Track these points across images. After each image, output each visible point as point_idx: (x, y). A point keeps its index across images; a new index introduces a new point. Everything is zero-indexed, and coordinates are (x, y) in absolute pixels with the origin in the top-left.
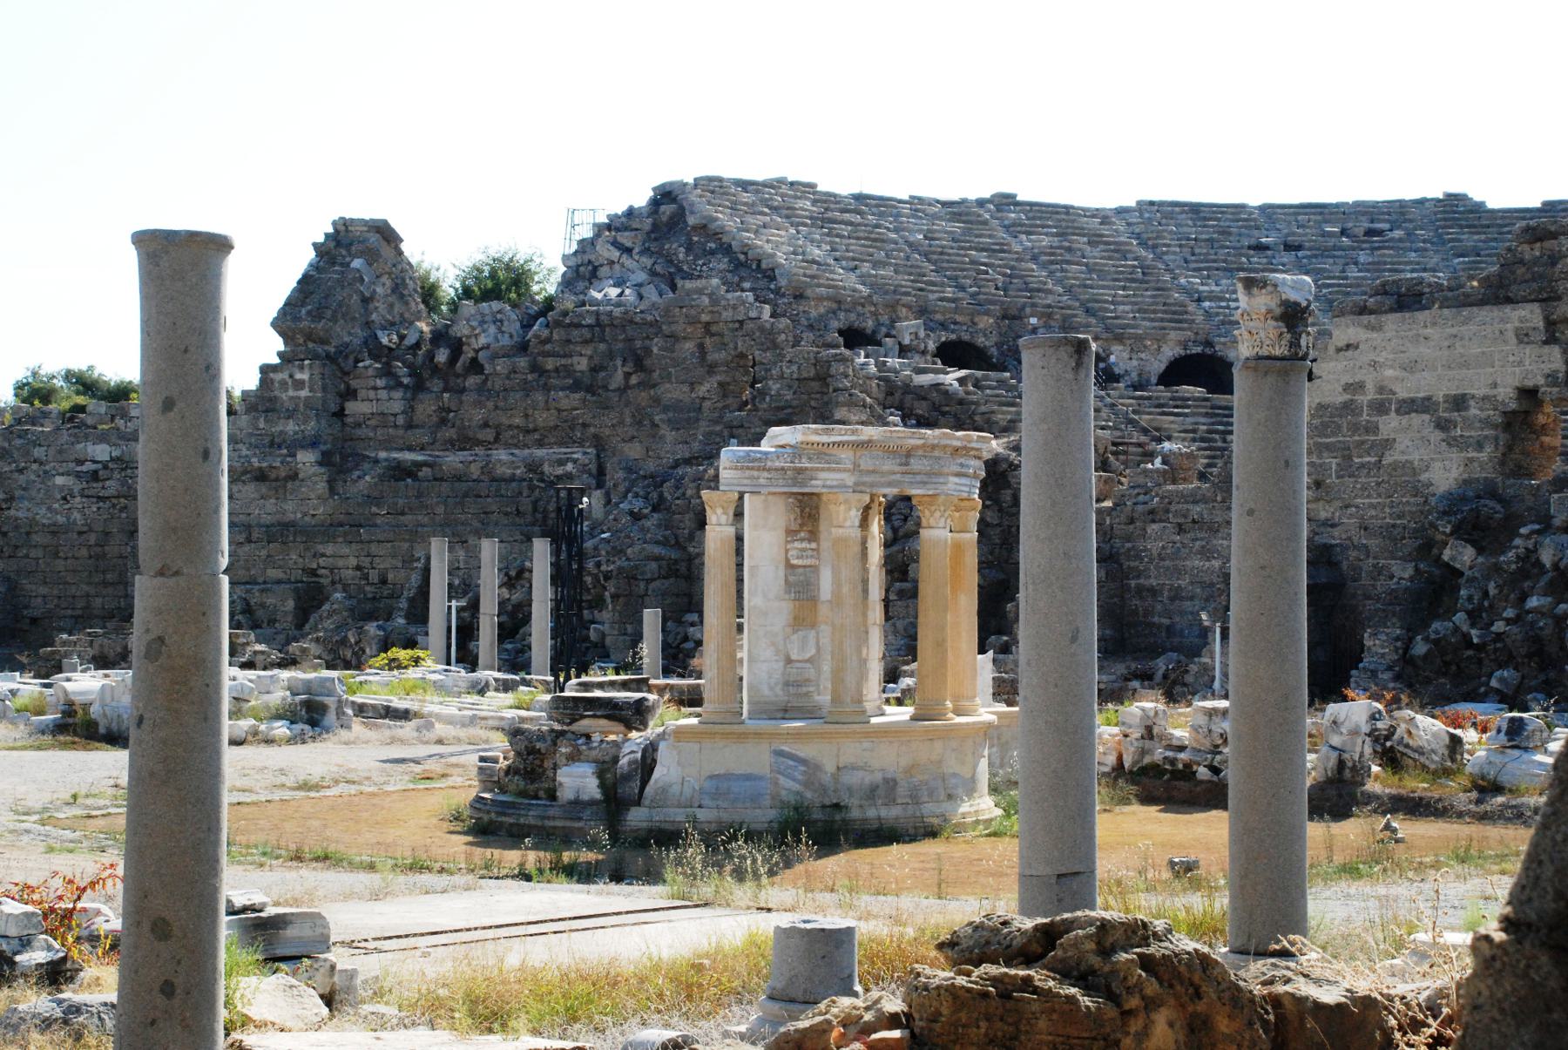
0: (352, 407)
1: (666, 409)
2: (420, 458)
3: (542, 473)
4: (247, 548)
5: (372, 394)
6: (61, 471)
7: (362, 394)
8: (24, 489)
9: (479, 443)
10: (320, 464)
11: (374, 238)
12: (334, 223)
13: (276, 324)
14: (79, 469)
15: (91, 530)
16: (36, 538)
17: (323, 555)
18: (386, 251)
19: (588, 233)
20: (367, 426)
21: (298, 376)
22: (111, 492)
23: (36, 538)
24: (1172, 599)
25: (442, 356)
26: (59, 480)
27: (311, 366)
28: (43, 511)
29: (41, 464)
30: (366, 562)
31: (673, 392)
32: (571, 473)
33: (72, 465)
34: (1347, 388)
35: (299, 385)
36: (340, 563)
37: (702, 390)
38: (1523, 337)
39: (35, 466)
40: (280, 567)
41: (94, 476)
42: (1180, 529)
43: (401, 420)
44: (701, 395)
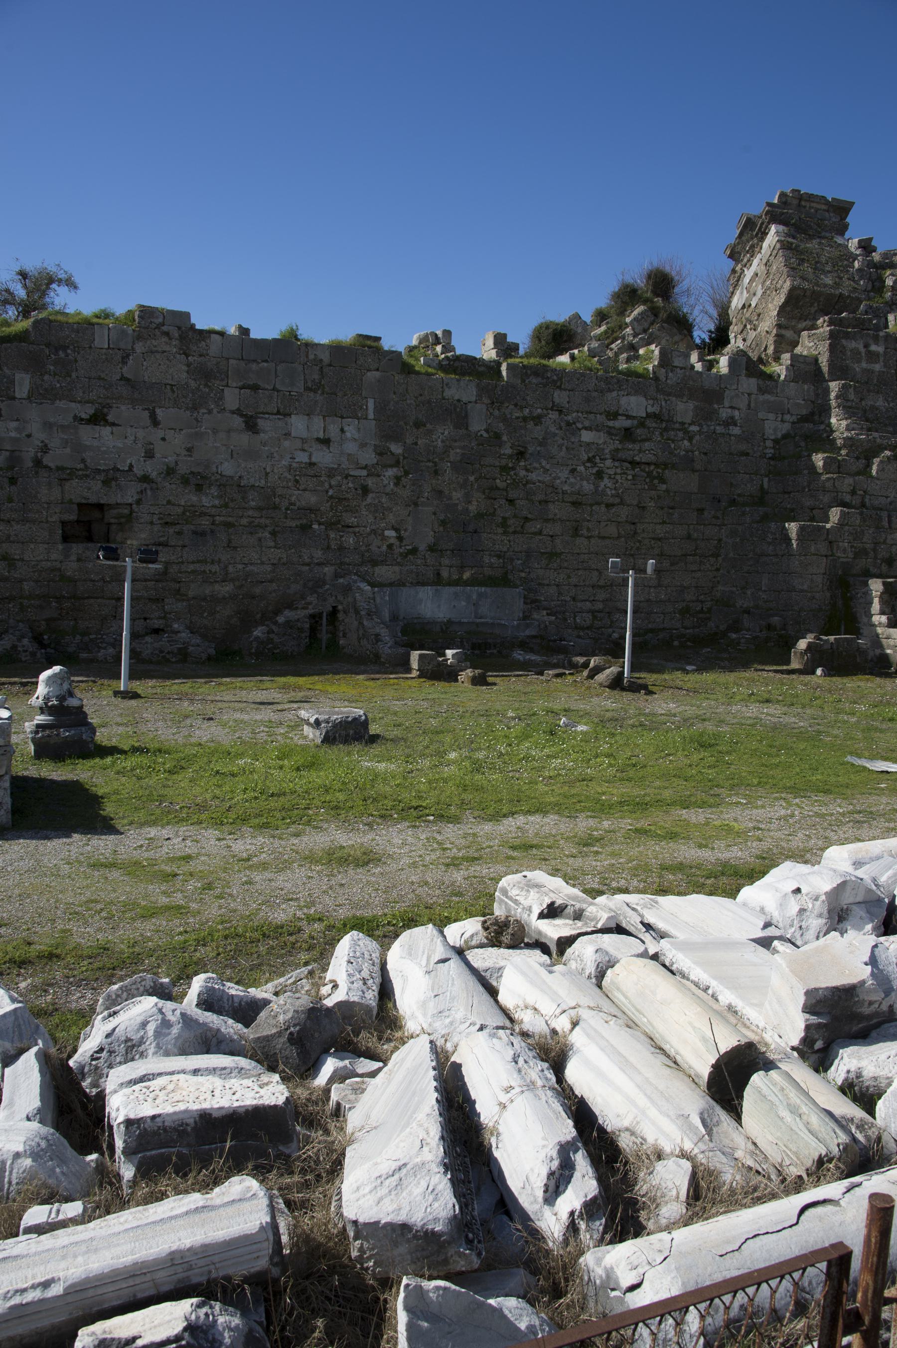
6: (587, 424)
8: (541, 444)
12: (783, 195)
14: (611, 424)
15: (622, 503)
16: (554, 509)
21: (873, 348)
22: (651, 458)
23: (554, 509)
26: (587, 436)
28: (564, 474)
29: (560, 412)
33: (601, 418)
35: (872, 357)
39: (554, 415)
41: (628, 434)
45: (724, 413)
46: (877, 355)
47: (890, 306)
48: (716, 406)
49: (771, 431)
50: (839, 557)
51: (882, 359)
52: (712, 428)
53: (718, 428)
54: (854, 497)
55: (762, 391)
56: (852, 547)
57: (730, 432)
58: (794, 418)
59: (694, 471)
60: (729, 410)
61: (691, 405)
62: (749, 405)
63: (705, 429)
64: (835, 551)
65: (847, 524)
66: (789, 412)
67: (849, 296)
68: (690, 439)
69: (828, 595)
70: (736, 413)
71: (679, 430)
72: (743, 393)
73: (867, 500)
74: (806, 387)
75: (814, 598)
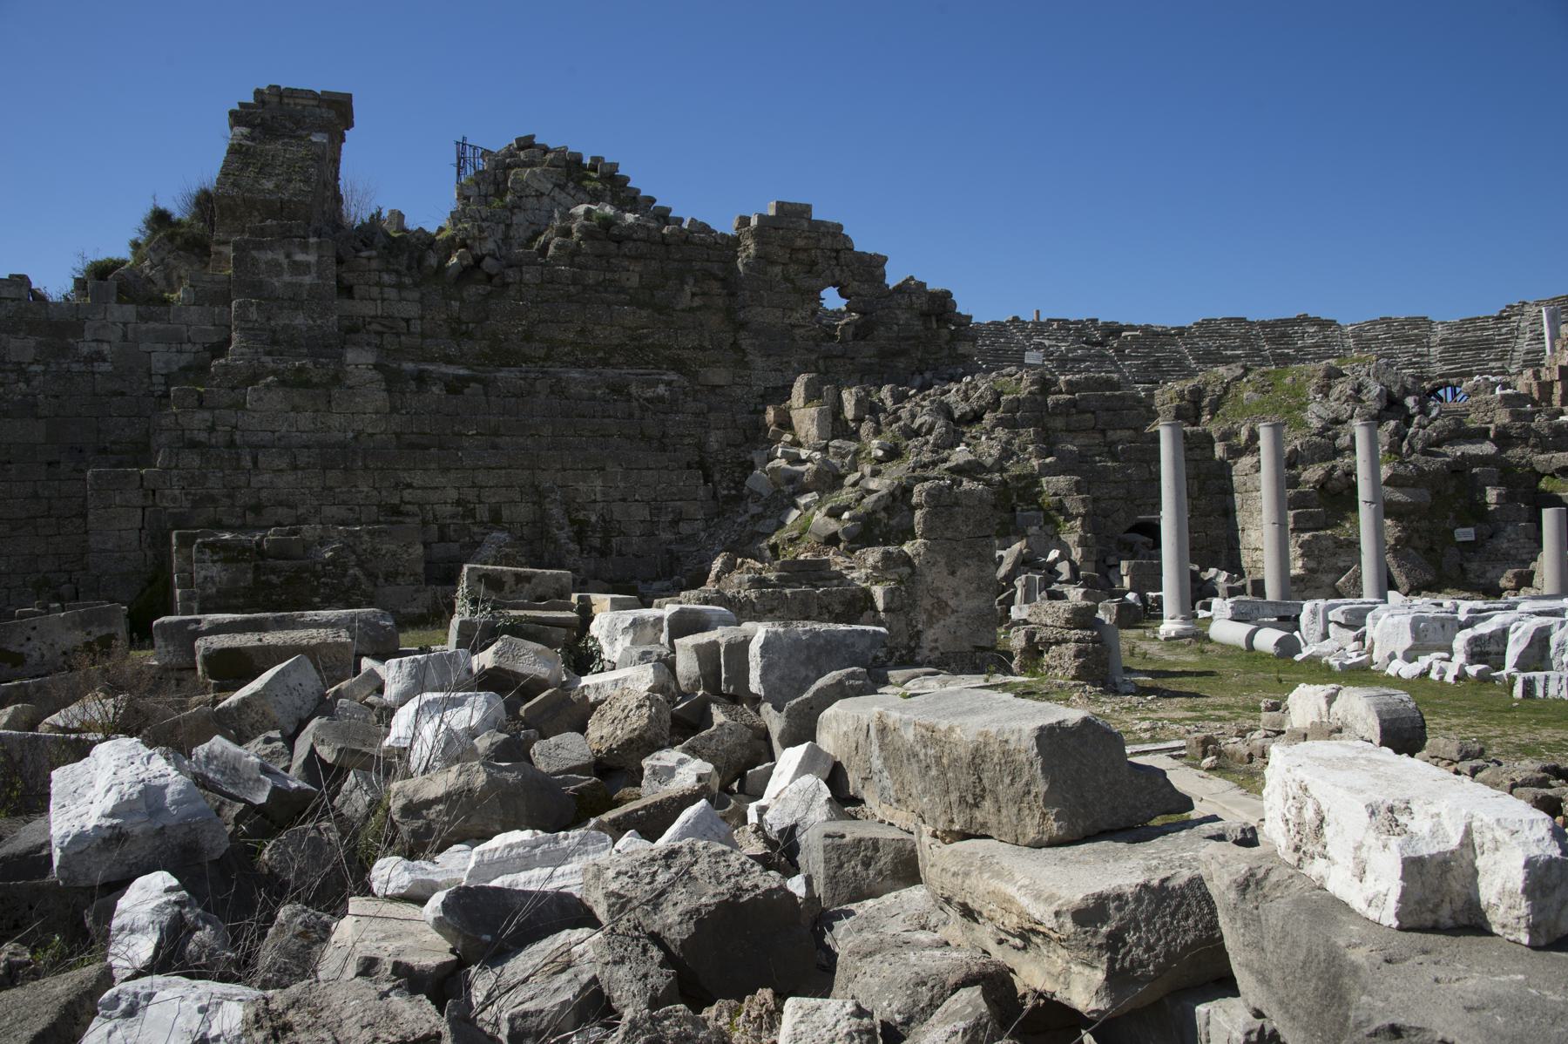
0: (347, 306)
2: (461, 372)
3: (629, 394)
4: (290, 477)
5: (375, 291)
7: (358, 291)
9: (527, 359)
10: (376, 367)
12: (258, 93)
17: (409, 486)
20: (368, 332)
21: (300, 257)
27: (319, 246)
30: (471, 495)
32: (663, 396)
36: (434, 496)
37: (796, 316)
40: (344, 503)
44: (792, 321)
45: (85, 349)
46: (308, 265)
47: (511, 211)
48: (71, 340)
49: (161, 365)
50: (165, 508)
51: (314, 269)
52: (65, 366)
53: (74, 365)
54: (214, 434)
55: (141, 318)
56: (186, 494)
57: (95, 369)
58: (199, 347)
59: (38, 418)
60: (94, 344)
61: (32, 341)
62: (125, 337)
63: (54, 367)
64: (157, 501)
65: (176, 467)
66: (189, 341)
67: (290, 201)
68: (28, 382)
69: (150, 553)
70: (106, 347)
71: (12, 371)
72: (114, 323)
73: (237, 437)
74: (217, 310)
75: (125, 558)
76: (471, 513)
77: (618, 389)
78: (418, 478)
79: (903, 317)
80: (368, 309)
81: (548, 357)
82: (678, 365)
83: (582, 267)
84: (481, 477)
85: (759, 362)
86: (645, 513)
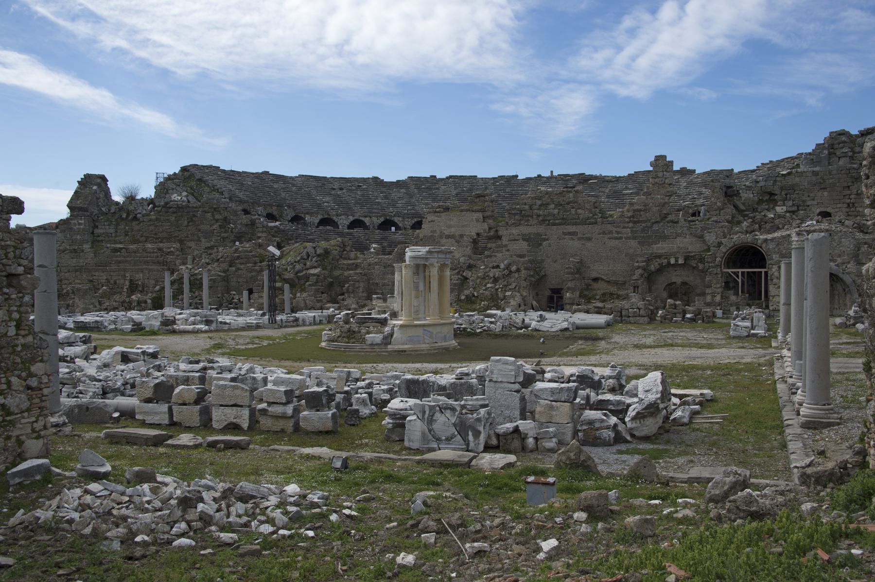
0: (96, 231)
1: (202, 233)
5: (103, 227)
11: (99, 180)
12: (84, 175)
13: (68, 206)
18: (103, 185)
19: (162, 180)
24: (383, 286)
25: (124, 216)
30: (109, 277)
31: (205, 227)
34: (432, 232)
35: (80, 224)
37: (214, 227)
38: (477, 221)
42: (385, 267)
43: (114, 235)
76: (109, 282)
77: (160, 249)
78: (97, 274)
79: (239, 227)
80: (102, 231)
81: (146, 241)
82: (181, 242)
83: (161, 216)
84: (112, 274)
85: (203, 240)
86: (154, 282)
